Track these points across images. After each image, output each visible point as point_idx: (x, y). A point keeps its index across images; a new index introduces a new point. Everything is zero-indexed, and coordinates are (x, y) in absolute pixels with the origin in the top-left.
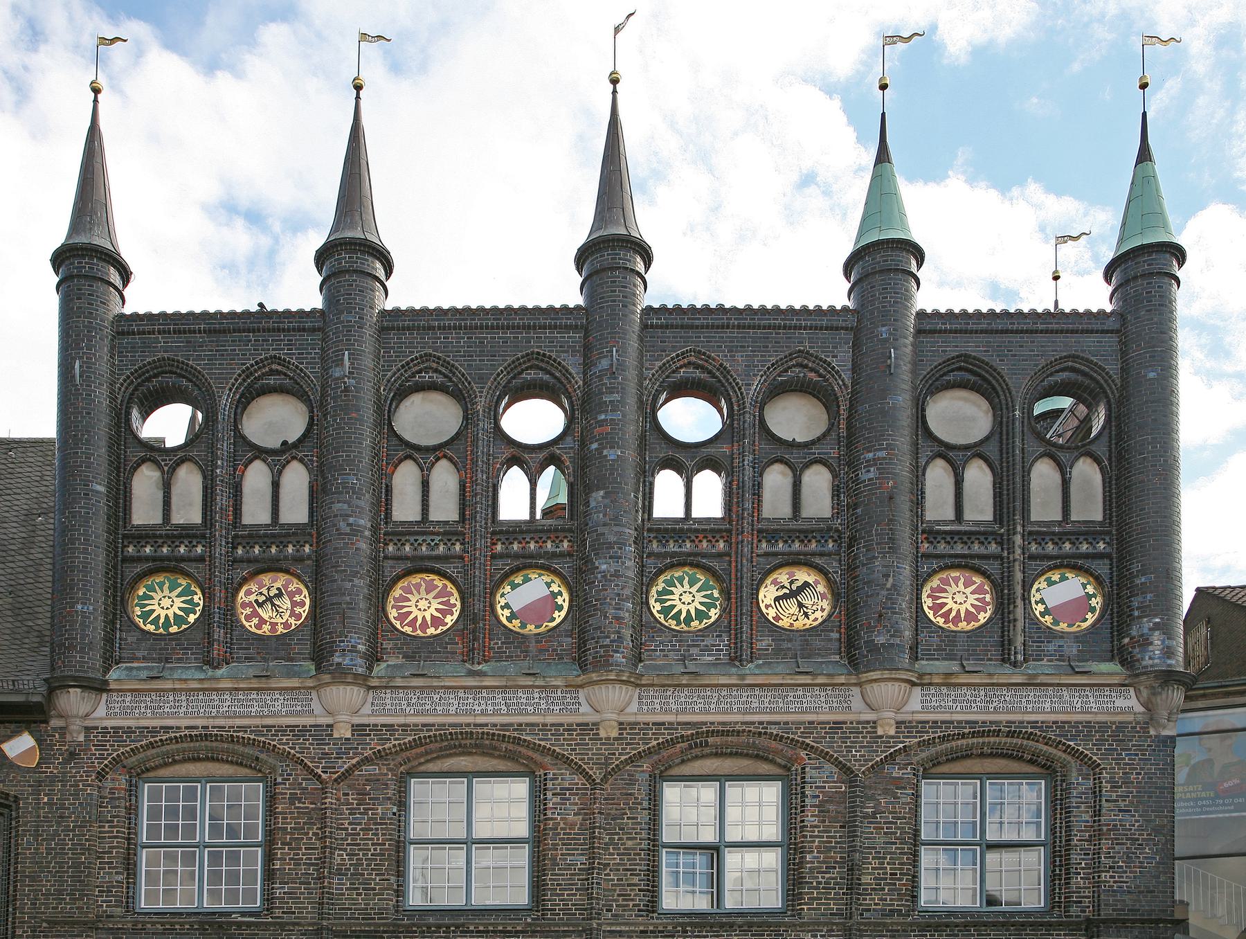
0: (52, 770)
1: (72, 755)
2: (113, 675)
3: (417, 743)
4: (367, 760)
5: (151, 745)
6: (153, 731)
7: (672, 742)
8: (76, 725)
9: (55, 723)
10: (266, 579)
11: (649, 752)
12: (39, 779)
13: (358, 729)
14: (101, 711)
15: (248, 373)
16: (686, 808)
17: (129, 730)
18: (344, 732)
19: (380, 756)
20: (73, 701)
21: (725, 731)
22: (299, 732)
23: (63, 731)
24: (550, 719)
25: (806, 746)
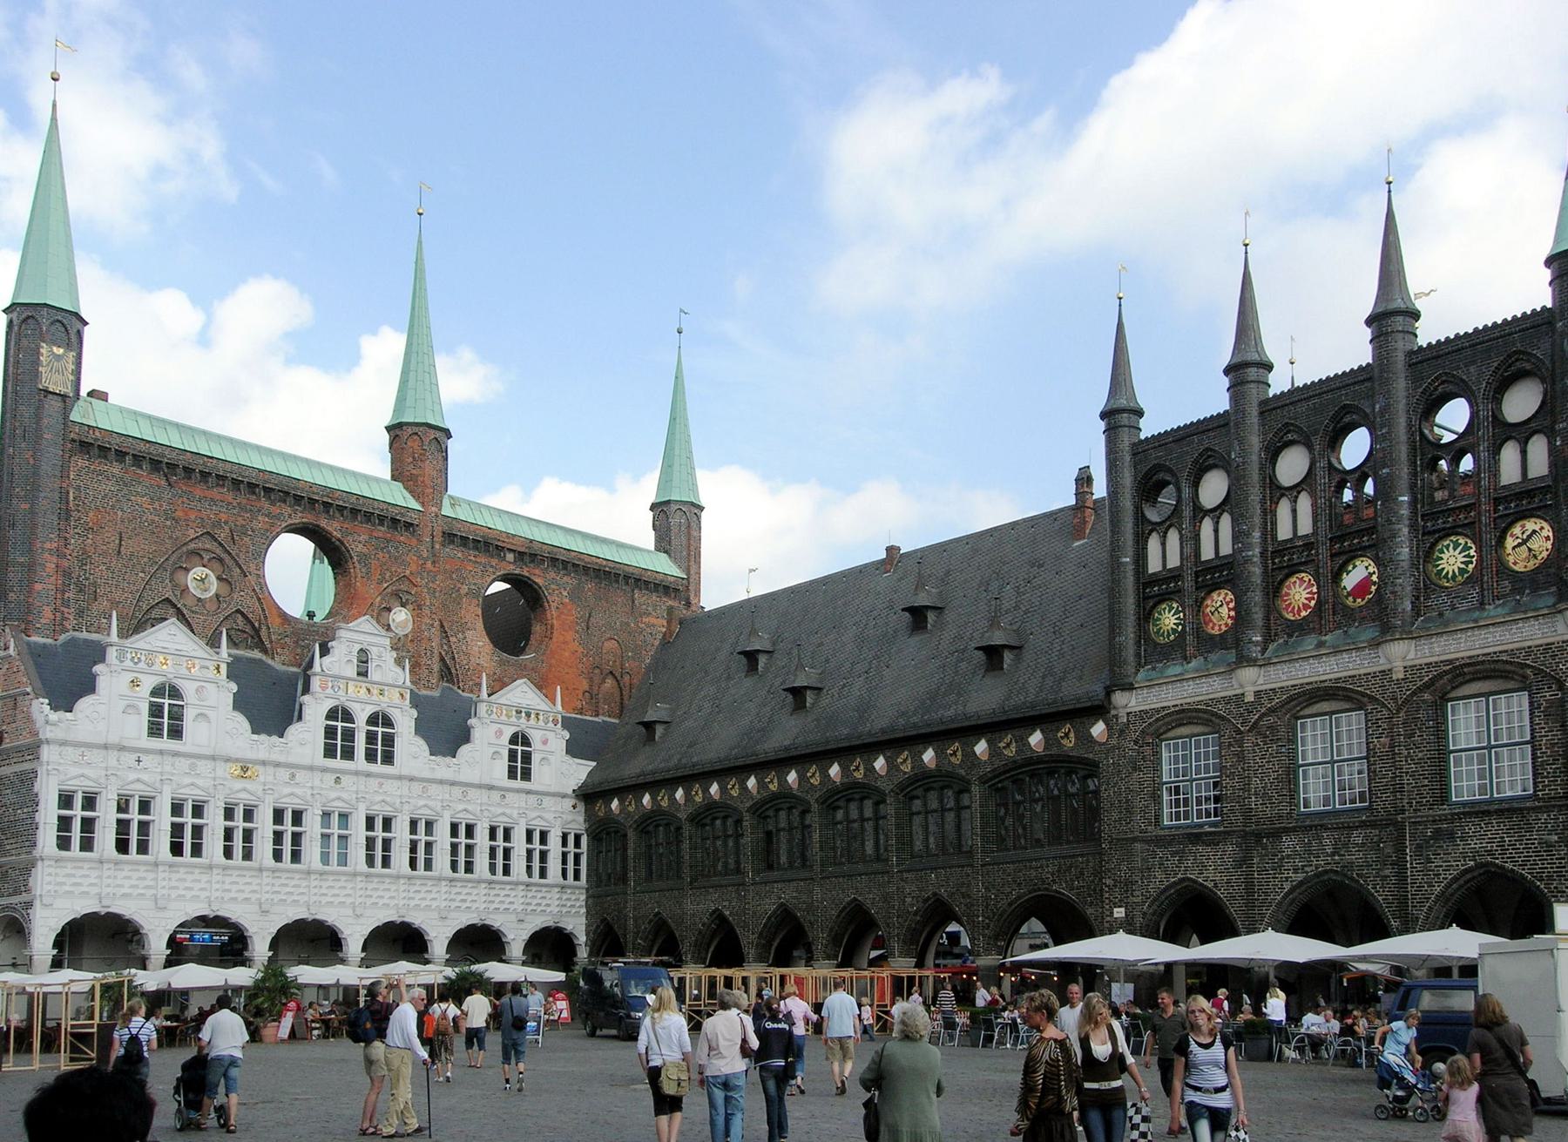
0: (1114, 742)
1: (1122, 732)
2: (1140, 676)
3: (1291, 699)
4: (1264, 715)
5: (1158, 720)
6: (1158, 711)
7: (1440, 676)
8: (1122, 713)
9: (1113, 712)
10: (1214, 595)
11: (1427, 686)
12: (1108, 749)
13: (1257, 693)
14: (1133, 703)
15: (1196, 462)
16: (1465, 723)
17: (1146, 712)
18: (1250, 698)
19: (1272, 711)
20: (1119, 698)
21: (1473, 663)
22: (1227, 700)
23: (1116, 717)
24: (1362, 671)
25: (1529, 666)
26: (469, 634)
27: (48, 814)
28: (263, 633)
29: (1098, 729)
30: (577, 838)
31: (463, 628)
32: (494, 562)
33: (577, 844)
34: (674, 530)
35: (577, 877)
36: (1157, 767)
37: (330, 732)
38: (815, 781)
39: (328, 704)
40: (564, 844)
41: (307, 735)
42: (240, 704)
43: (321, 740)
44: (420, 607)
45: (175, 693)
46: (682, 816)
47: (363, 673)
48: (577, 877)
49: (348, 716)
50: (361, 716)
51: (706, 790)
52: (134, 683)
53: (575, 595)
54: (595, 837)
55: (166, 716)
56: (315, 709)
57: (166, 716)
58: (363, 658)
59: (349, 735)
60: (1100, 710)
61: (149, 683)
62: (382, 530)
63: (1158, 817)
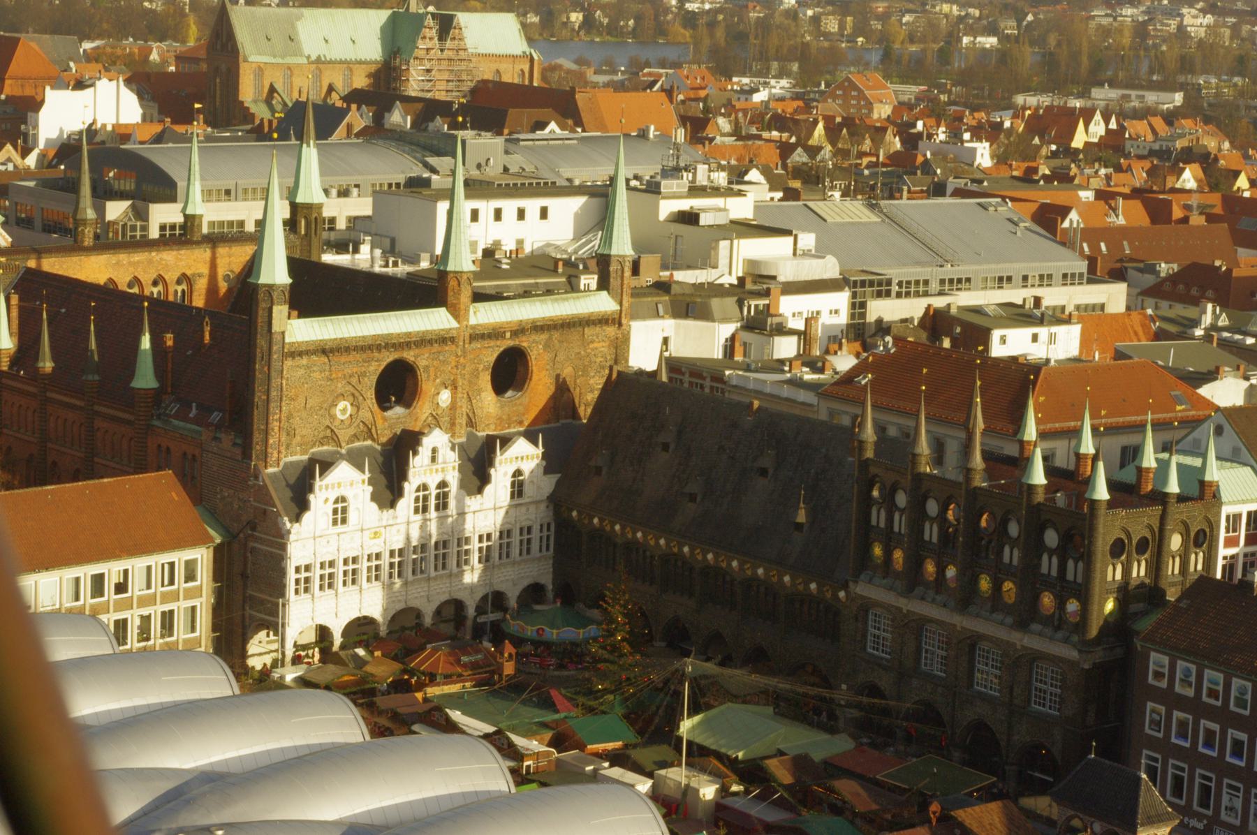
26: (483, 395)
27: (291, 576)
28: (373, 431)
29: (842, 594)
30: (549, 525)
31: (480, 391)
32: (498, 343)
33: (548, 529)
34: (613, 275)
35: (548, 549)
36: (866, 623)
37: (417, 499)
38: (700, 557)
39: (414, 486)
40: (541, 531)
41: (406, 504)
42: (375, 498)
43: (412, 505)
44: (456, 388)
45: (343, 499)
46: (619, 541)
47: (433, 459)
48: (548, 549)
49: (425, 487)
50: (433, 486)
51: (634, 533)
52: (326, 500)
53: (547, 346)
54: (558, 526)
55: (340, 515)
56: (410, 488)
57: (340, 515)
58: (434, 450)
59: (425, 498)
60: (845, 587)
61: (332, 499)
62: (436, 347)
63: (864, 648)
